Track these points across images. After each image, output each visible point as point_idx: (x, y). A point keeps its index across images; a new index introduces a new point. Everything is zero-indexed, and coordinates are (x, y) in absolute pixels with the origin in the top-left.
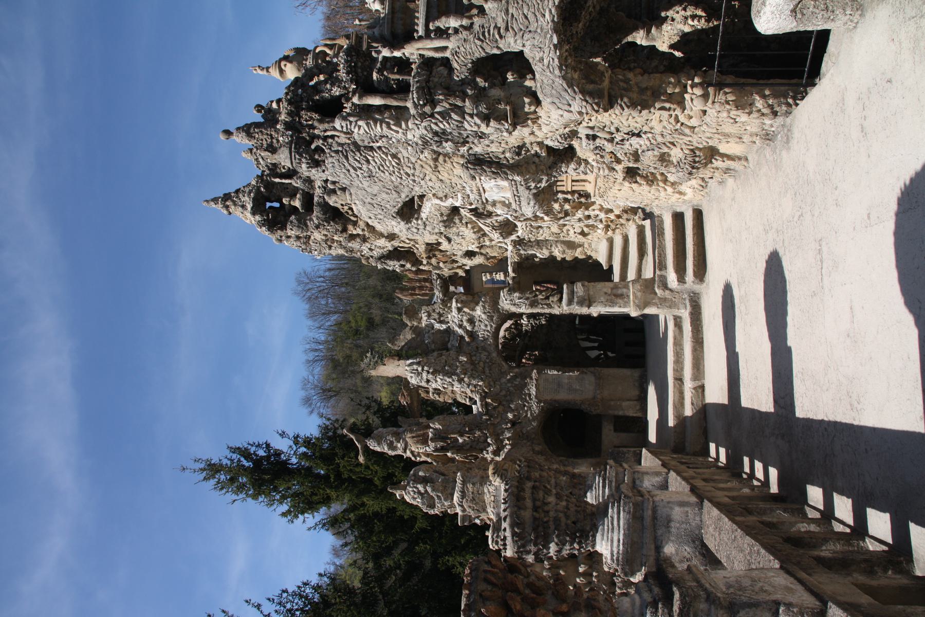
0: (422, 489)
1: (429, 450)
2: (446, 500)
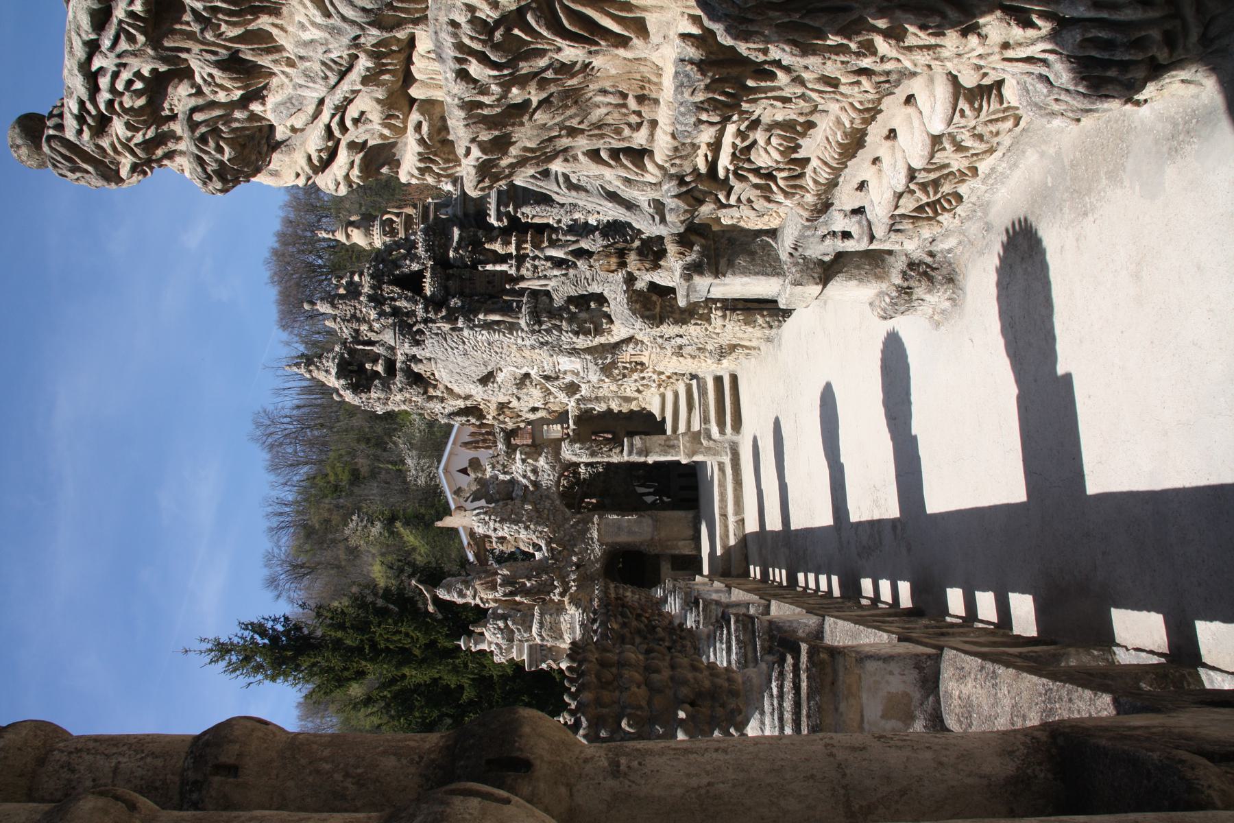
2: (525, 632)
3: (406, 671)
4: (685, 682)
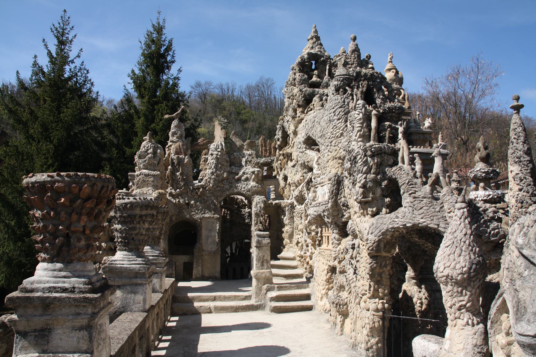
0: (149, 151)
1: (172, 155)
2: (144, 165)
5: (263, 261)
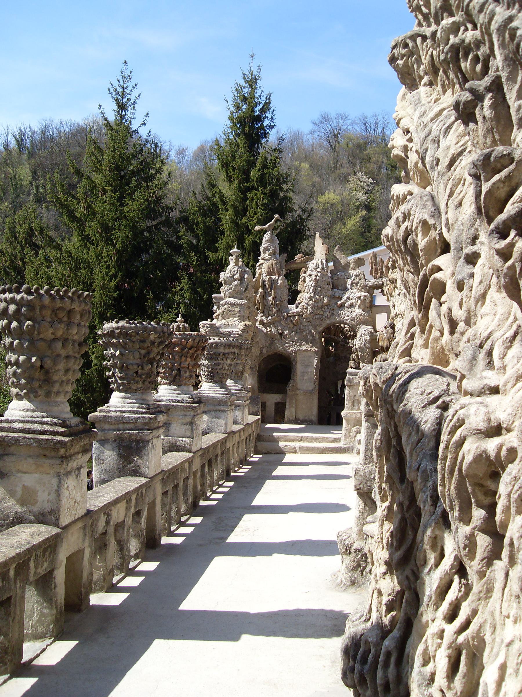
0: (236, 277)
2: (229, 293)
3: (230, 212)
4: (55, 363)
5: (354, 401)
